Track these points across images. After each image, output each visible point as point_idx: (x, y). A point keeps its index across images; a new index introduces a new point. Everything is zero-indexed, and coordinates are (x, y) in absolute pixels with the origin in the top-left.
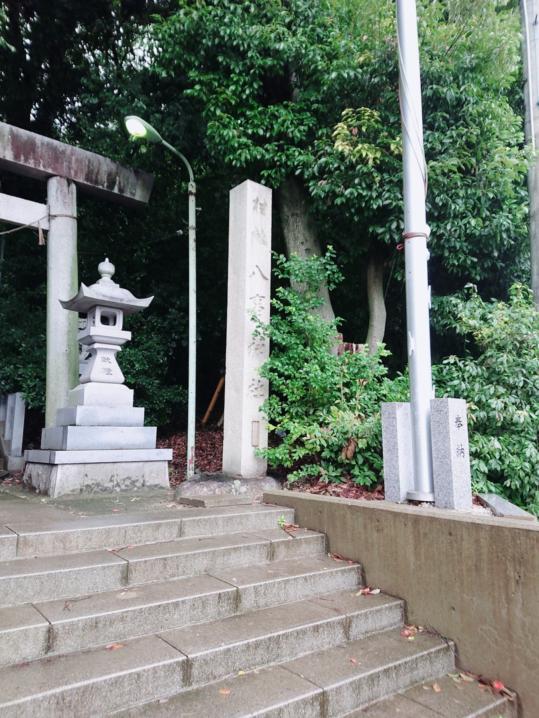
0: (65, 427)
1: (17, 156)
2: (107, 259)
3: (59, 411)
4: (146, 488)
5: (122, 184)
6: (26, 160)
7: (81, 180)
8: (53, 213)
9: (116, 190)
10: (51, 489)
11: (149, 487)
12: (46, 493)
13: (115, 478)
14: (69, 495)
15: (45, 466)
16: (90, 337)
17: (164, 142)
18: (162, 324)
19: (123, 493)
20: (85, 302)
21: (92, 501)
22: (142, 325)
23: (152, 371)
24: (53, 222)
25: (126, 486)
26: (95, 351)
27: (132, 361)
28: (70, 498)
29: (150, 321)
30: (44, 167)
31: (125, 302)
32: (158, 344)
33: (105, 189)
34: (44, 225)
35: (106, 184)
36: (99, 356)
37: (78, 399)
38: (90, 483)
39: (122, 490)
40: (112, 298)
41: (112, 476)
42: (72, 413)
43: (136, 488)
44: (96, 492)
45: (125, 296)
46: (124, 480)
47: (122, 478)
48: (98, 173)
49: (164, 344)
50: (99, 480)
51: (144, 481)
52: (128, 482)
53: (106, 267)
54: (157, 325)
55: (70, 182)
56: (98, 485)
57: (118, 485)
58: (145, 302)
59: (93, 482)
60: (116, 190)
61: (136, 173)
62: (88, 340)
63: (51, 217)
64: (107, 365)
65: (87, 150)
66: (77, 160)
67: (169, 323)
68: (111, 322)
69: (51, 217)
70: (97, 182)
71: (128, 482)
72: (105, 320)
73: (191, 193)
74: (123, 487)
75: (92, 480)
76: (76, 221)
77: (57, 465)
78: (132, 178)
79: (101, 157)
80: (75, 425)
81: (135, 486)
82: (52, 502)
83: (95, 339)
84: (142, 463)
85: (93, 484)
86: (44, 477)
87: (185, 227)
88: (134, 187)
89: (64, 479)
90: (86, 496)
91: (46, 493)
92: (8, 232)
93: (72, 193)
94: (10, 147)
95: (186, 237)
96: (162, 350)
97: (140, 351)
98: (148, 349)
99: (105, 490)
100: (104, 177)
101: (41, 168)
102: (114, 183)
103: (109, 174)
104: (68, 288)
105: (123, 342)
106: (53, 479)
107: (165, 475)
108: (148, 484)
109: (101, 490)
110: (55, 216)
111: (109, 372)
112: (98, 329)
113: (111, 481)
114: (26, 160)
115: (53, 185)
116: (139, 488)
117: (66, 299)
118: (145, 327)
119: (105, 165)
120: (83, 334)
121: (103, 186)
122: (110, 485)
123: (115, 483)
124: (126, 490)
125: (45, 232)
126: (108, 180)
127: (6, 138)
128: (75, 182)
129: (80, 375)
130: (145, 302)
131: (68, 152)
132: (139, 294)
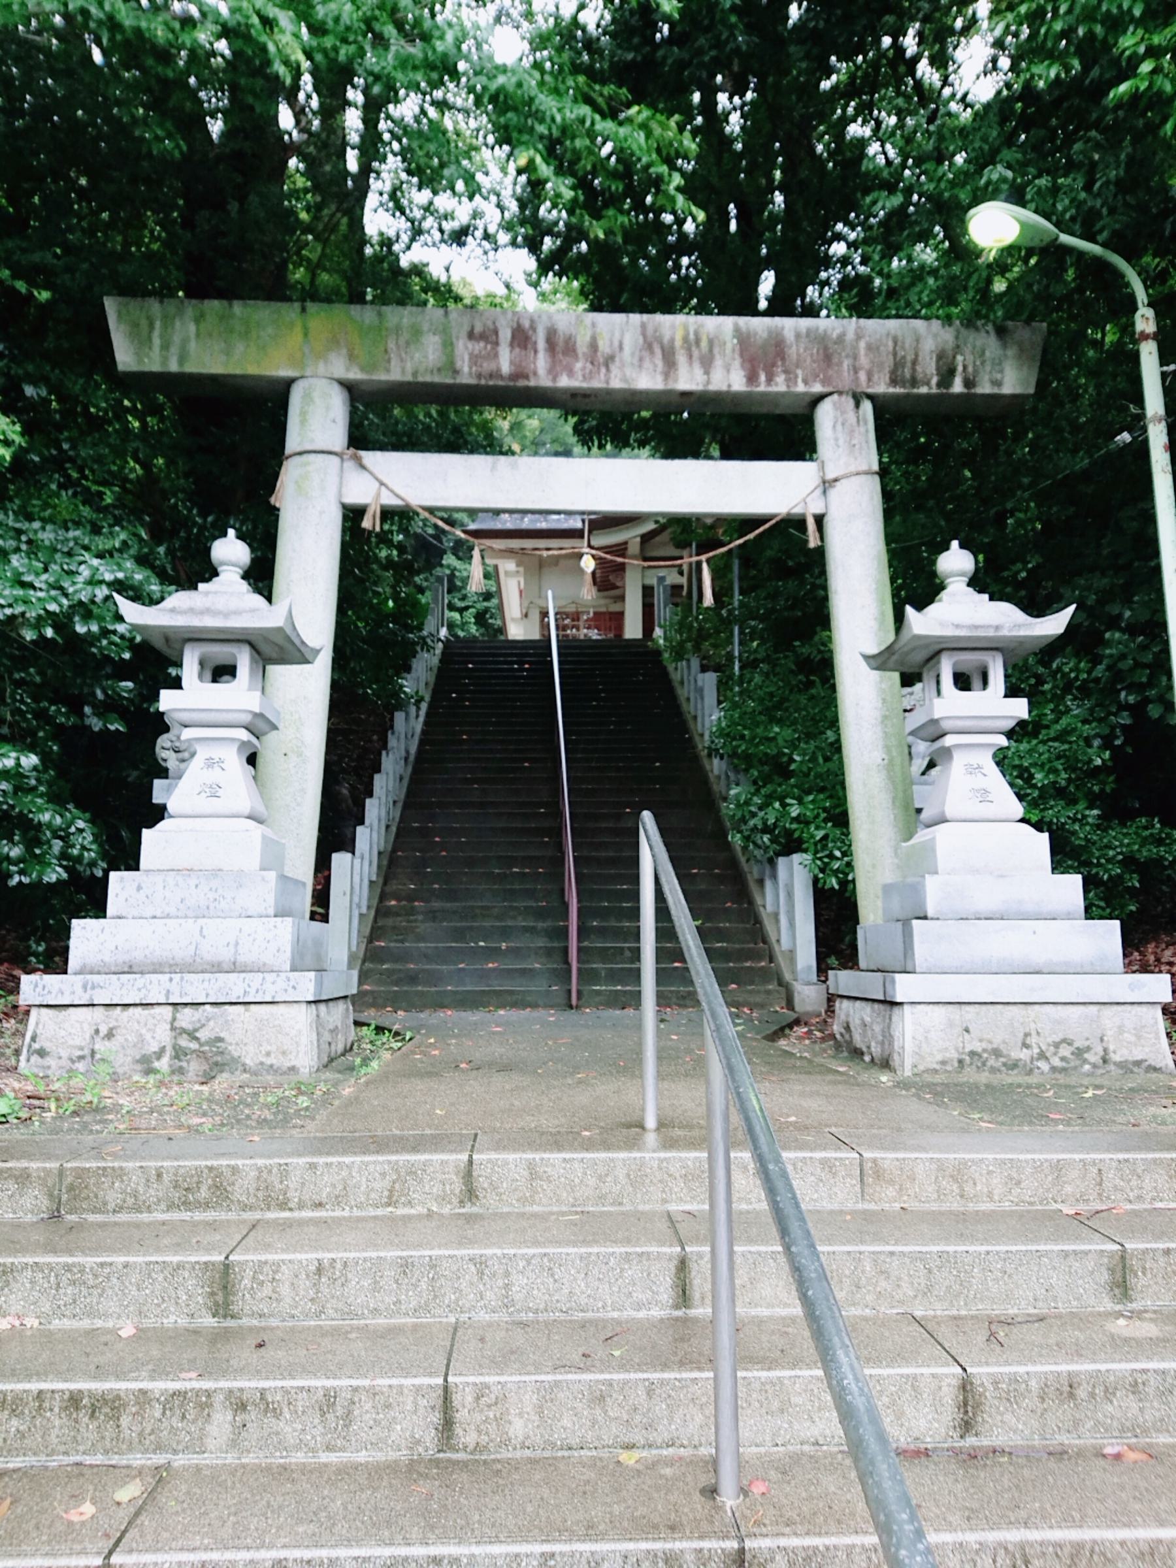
0: (906, 923)
1: (752, 378)
2: (955, 544)
3: (887, 889)
4: (1112, 1067)
5: (970, 369)
6: (770, 380)
7: (882, 387)
8: (830, 476)
9: (958, 387)
10: (896, 1057)
11: (1119, 1065)
12: (885, 1064)
13: (1032, 1040)
14: (936, 1071)
15: (876, 1006)
16: (934, 722)
17: (1065, 238)
18: (1089, 673)
19: (1057, 1075)
20: (913, 649)
21: (990, 1089)
22: (1040, 681)
23: (1077, 788)
24: (833, 493)
25: (1063, 1059)
26: (947, 752)
27: (1027, 769)
28: (938, 1079)
29: (1059, 669)
30: (806, 382)
31: (1005, 632)
32: (1085, 722)
33: (934, 390)
34: (815, 507)
35: (934, 380)
36: (959, 761)
37: (922, 863)
38: (978, 1047)
39: (1054, 1069)
40: (976, 627)
41: (1027, 1035)
42: (915, 892)
43: (1087, 1067)
44: (993, 1070)
45: (1005, 619)
46: (1057, 1045)
47: (1050, 1040)
48: (914, 362)
49: (1100, 720)
50: (997, 1042)
51: (1105, 1050)
52: (1065, 1051)
53: (956, 561)
54: (1077, 678)
55: (857, 399)
56: (997, 1053)
57: (1042, 1056)
58: (1055, 624)
59: (984, 1045)
60: (958, 387)
61: (1001, 332)
62: (931, 731)
63: (827, 485)
64: (979, 782)
65: (888, 317)
66: (869, 348)
67: (1109, 668)
68: (976, 682)
69: (827, 485)
70: (914, 382)
71: (1065, 1051)
72: (962, 682)
73: (1145, 337)
74: (1056, 1062)
75: (981, 1041)
76: (877, 479)
77: (901, 1004)
78: (988, 341)
79: (918, 323)
80: (925, 918)
81: (1085, 1061)
82: (904, 1085)
83: (946, 725)
84: (1094, 1008)
85: (985, 1050)
86: (877, 1028)
87: (1138, 424)
88: (998, 364)
89: (922, 1035)
90: (970, 1075)
91: (885, 1064)
92: (751, 536)
93: (866, 423)
94: (737, 363)
95: (1141, 450)
96: (1097, 735)
97: (1044, 742)
98: (1061, 737)
99: (1014, 1065)
100: (929, 367)
101: (801, 388)
102: (952, 372)
103: (940, 357)
104: (873, 624)
105: (1011, 724)
106: (897, 1034)
107: (1158, 1038)
108: (1117, 1058)
109: (1004, 1064)
110: (836, 480)
111: (984, 795)
112: (948, 703)
113: (1025, 1045)
114: (770, 380)
115: (826, 418)
116: (1095, 1066)
117: (873, 650)
118: (1047, 687)
119: (925, 337)
120: (916, 720)
121: (928, 384)
122: (1024, 1055)
123: (1036, 1051)
124: (1064, 1069)
125: (820, 520)
126: (938, 369)
127: (729, 346)
128: (870, 397)
129: (919, 811)
130: (1055, 624)
131: (850, 335)
132: (1036, 607)
